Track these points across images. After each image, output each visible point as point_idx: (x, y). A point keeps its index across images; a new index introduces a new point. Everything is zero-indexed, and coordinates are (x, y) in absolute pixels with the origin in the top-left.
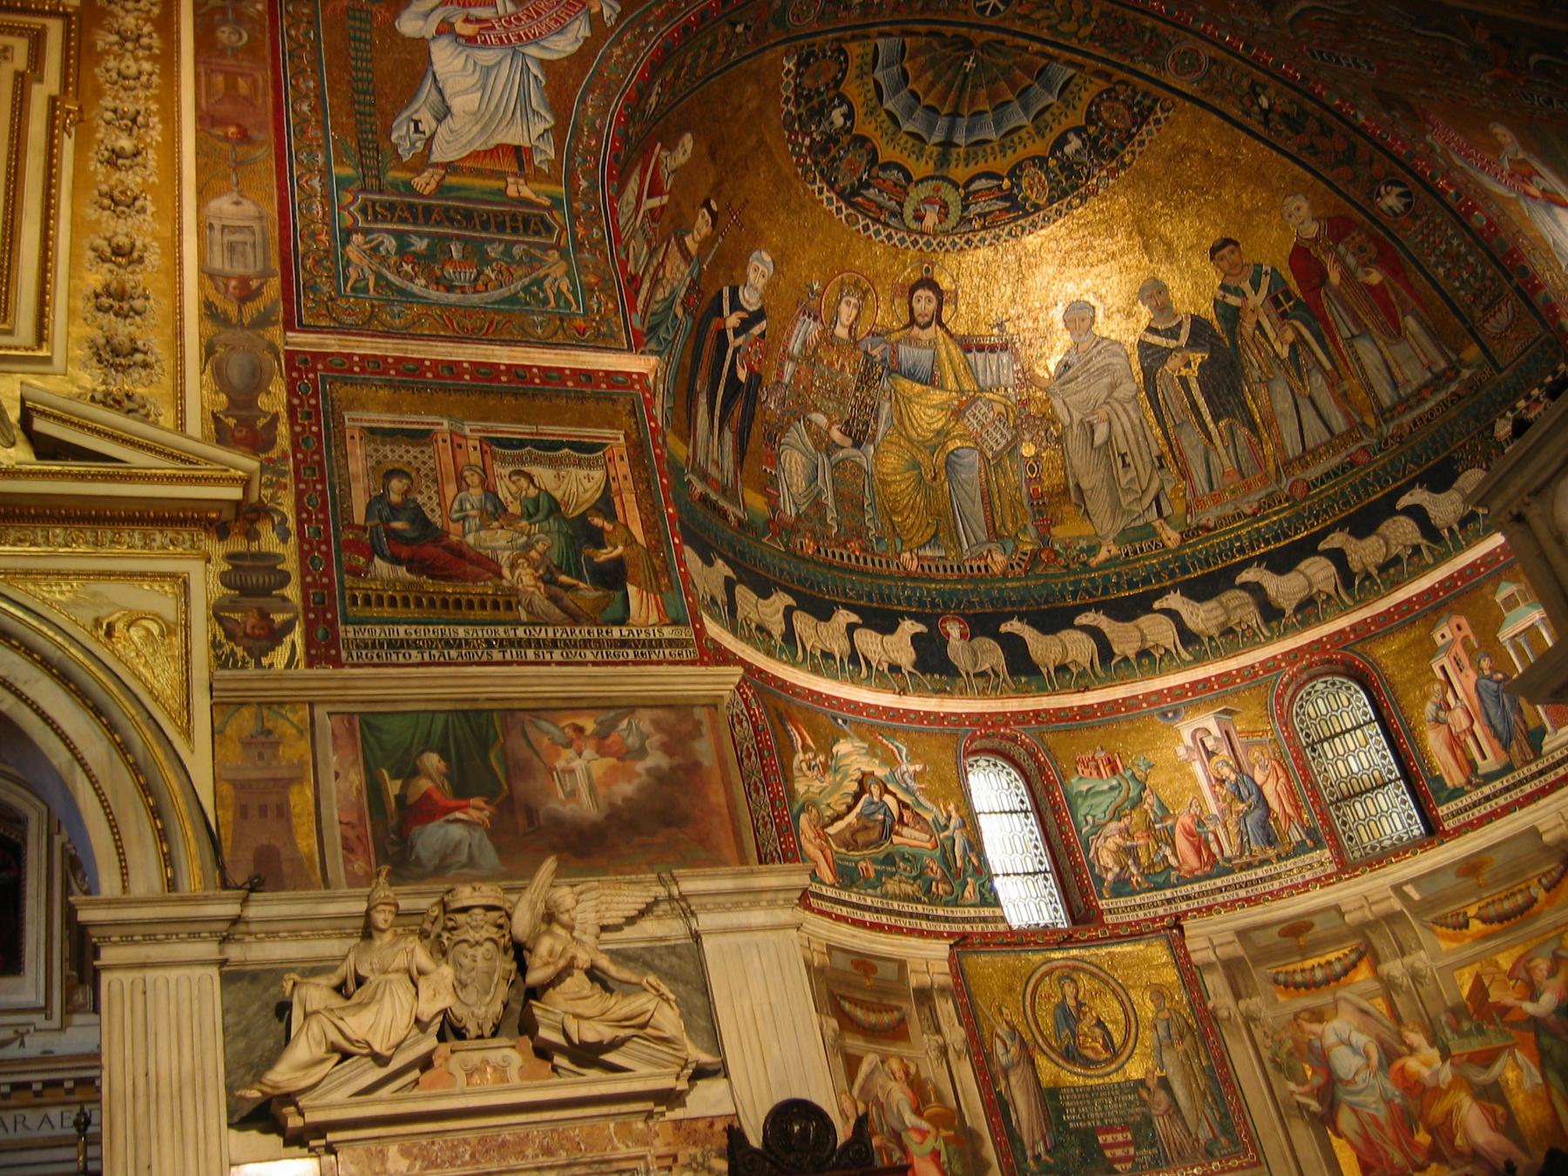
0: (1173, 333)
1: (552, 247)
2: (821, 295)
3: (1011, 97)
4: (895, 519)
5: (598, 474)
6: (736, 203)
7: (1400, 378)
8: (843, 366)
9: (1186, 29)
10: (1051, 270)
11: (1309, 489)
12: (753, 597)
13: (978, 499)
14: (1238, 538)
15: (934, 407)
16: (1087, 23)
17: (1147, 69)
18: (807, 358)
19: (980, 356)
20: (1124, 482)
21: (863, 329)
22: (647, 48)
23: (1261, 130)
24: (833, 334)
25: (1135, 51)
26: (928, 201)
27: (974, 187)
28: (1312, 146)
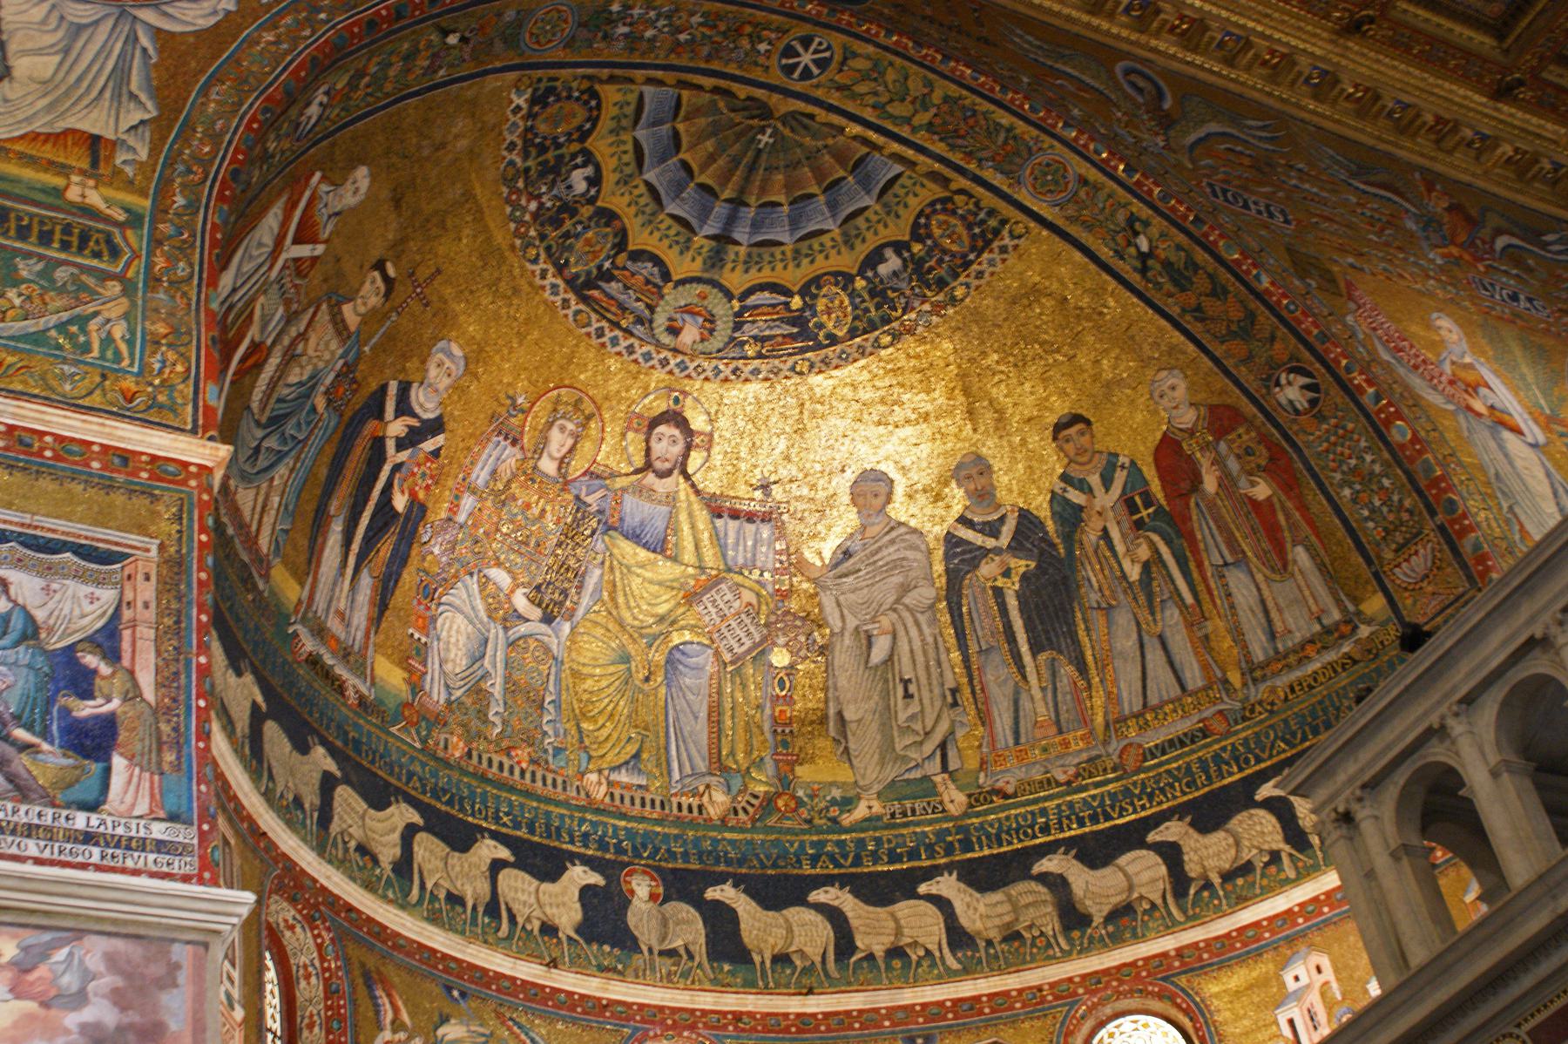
0: (992, 530)
1: (113, 277)
2: (526, 412)
3: (815, 189)
4: (584, 725)
5: (108, 595)
6: (423, 273)
7: (1279, 627)
8: (543, 511)
9: (1054, 136)
10: (842, 424)
11: (1145, 760)
12: (361, 805)
13: (703, 714)
15: (660, 584)
16: (926, 109)
17: (998, 180)
18: (497, 493)
19: (733, 525)
20: (902, 716)
21: (577, 466)
22: (311, 41)
23: (1135, 278)
24: (535, 468)
25: (984, 154)
26: (687, 310)
27: (752, 300)
28: (1198, 309)
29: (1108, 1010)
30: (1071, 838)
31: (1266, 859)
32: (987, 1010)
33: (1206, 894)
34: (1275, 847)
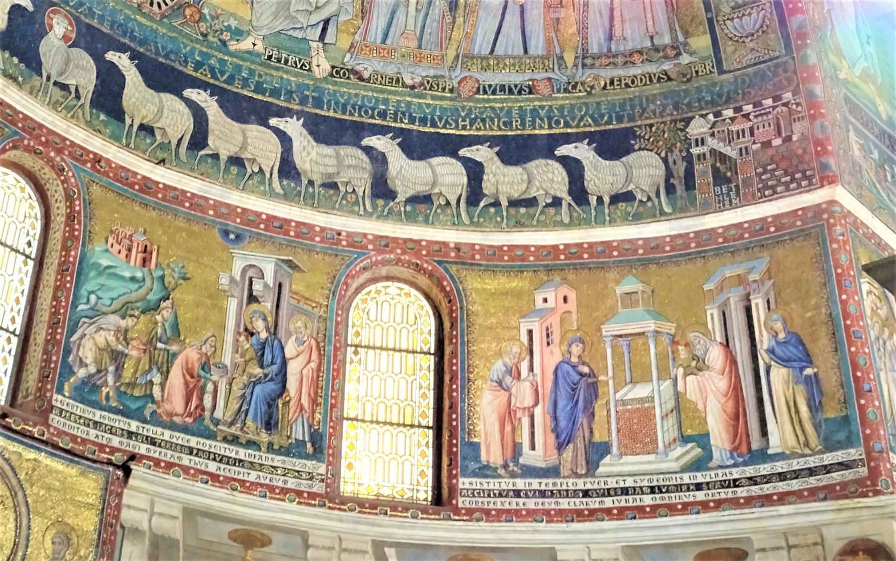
11: (478, 92)
14: (386, 102)
29: (384, 271)
30: (402, 130)
31: (549, 201)
32: (292, 233)
33: (492, 210)
34: (559, 195)
